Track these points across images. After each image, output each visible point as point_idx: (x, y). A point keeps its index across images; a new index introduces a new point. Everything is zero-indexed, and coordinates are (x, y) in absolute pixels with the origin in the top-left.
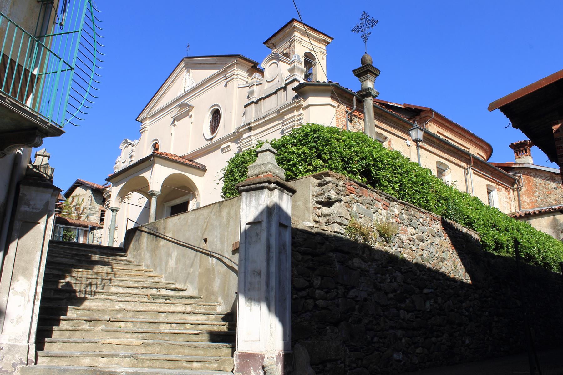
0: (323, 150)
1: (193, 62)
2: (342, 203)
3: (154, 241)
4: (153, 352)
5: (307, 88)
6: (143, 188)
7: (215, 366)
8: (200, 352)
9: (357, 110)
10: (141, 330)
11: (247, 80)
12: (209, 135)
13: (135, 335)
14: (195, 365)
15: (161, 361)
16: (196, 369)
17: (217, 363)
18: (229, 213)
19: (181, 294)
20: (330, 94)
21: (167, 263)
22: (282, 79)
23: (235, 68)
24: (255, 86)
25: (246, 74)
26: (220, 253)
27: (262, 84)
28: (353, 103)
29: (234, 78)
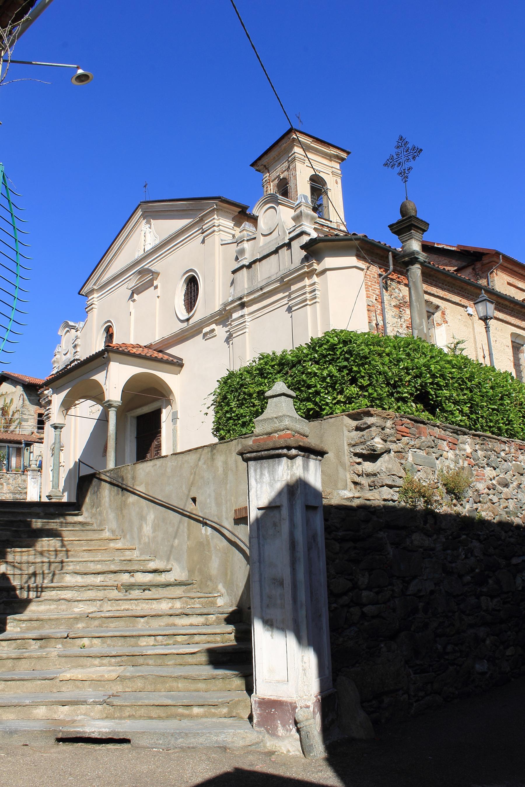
0: (359, 372)
1: (153, 210)
2: (392, 453)
3: (120, 496)
4: (134, 689)
5: (321, 245)
6: (96, 394)
7: (225, 710)
8: (201, 686)
9: (394, 271)
10: (114, 653)
11: (233, 232)
12: (183, 314)
13: (106, 661)
14: (196, 710)
15: (146, 708)
16: (197, 716)
17: (228, 706)
18: (226, 463)
19: (162, 578)
20: (355, 252)
21: (140, 528)
22: (284, 232)
23: (215, 216)
24: (245, 242)
25: (231, 224)
26: (216, 520)
27: (255, 238)
28: (388, 262)
29: (214, 231)
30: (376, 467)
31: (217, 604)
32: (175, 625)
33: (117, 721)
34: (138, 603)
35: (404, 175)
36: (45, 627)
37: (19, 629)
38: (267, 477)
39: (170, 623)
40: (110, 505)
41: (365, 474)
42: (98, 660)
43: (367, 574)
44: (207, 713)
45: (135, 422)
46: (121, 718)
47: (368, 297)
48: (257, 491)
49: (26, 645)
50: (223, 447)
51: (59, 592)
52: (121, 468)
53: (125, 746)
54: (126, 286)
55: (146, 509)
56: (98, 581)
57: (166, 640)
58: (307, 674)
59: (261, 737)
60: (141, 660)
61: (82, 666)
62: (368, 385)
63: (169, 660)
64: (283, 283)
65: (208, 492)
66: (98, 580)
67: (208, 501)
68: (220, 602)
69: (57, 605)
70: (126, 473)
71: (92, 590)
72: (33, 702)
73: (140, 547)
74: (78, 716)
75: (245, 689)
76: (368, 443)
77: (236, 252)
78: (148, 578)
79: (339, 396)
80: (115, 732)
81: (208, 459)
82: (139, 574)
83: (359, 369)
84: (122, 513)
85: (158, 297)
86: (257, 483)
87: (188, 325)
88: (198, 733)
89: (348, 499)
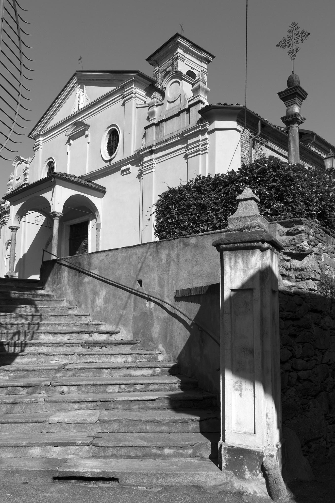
0: (286, 191)
1: (86, 78)
2: (313, 254)
3: (77, 277)
4: (111, 431)
5: (213, 110)
6: (44, 208)
7: (190, 451)
8: (165, 428)
9: (261, 136)
10: (91, 399)
11: (145, 99)
12: (107, 156)
13: (84, 405)
14: (167, 451)
15: (125, 449)
16: (168, 456)
17: (193, 448)
18: (169, 255)
19: (113, 338)
20: (236, 118)
21: (93, 301)
22: (185, 100)
23: (133, 86)
24: (155, 107)
25: (144, 93)
26: (159, 297)
27: (162, 104)
29: (132, 97)
30: (304, 264)
31: (158, 359)
32: (131, 376)
33: (102, 460)
34: (100, 357)
35: (292, 54)
36: (29, 376)
37: (7, 378)
38: (240, 264)
39: (127, 374)
40: (68, 283)
41: (293, 269)
42: (77, 404)
43: (301, 346)
44: (176, 453)
45: (69, 229)
46: (105, 457)
47: (242, 151)
48: (231, 276)
49: (15, 391)
50: (165, 243)
51: (37, 348)
52: (79, 256)
53: (113, 484)
54: (64, 133)
55: (99, 287)
56: (66, 339)
57: (128, 388)
58: (271, 428)
59: (229, 478)
60: (112, 405)
61: (65, 410)
62: (292, 202)
63: (134, 405)
64: (182, 138)
65: (153, 277)
66: (65, 338)
67: (152, 283)
68: (160, 358)
69: (37, 358)
70: (83, 260)
71: (62, 346)
72: (29, 443)
73: (93, 314)
74: (68, 455)
75: (199, 431)
76: (299, 245)
77: (148, 113)
78: (103, 337)
79: (267, 210)
80: (105, 473)
81: (153, 252)
82: (96, 334)
83: (285, 188)
84: (78, 289)
85: (89, 143)
86: (231, 269)
87: (110, 164)
88: (177, 474)
89: (289, 287)
